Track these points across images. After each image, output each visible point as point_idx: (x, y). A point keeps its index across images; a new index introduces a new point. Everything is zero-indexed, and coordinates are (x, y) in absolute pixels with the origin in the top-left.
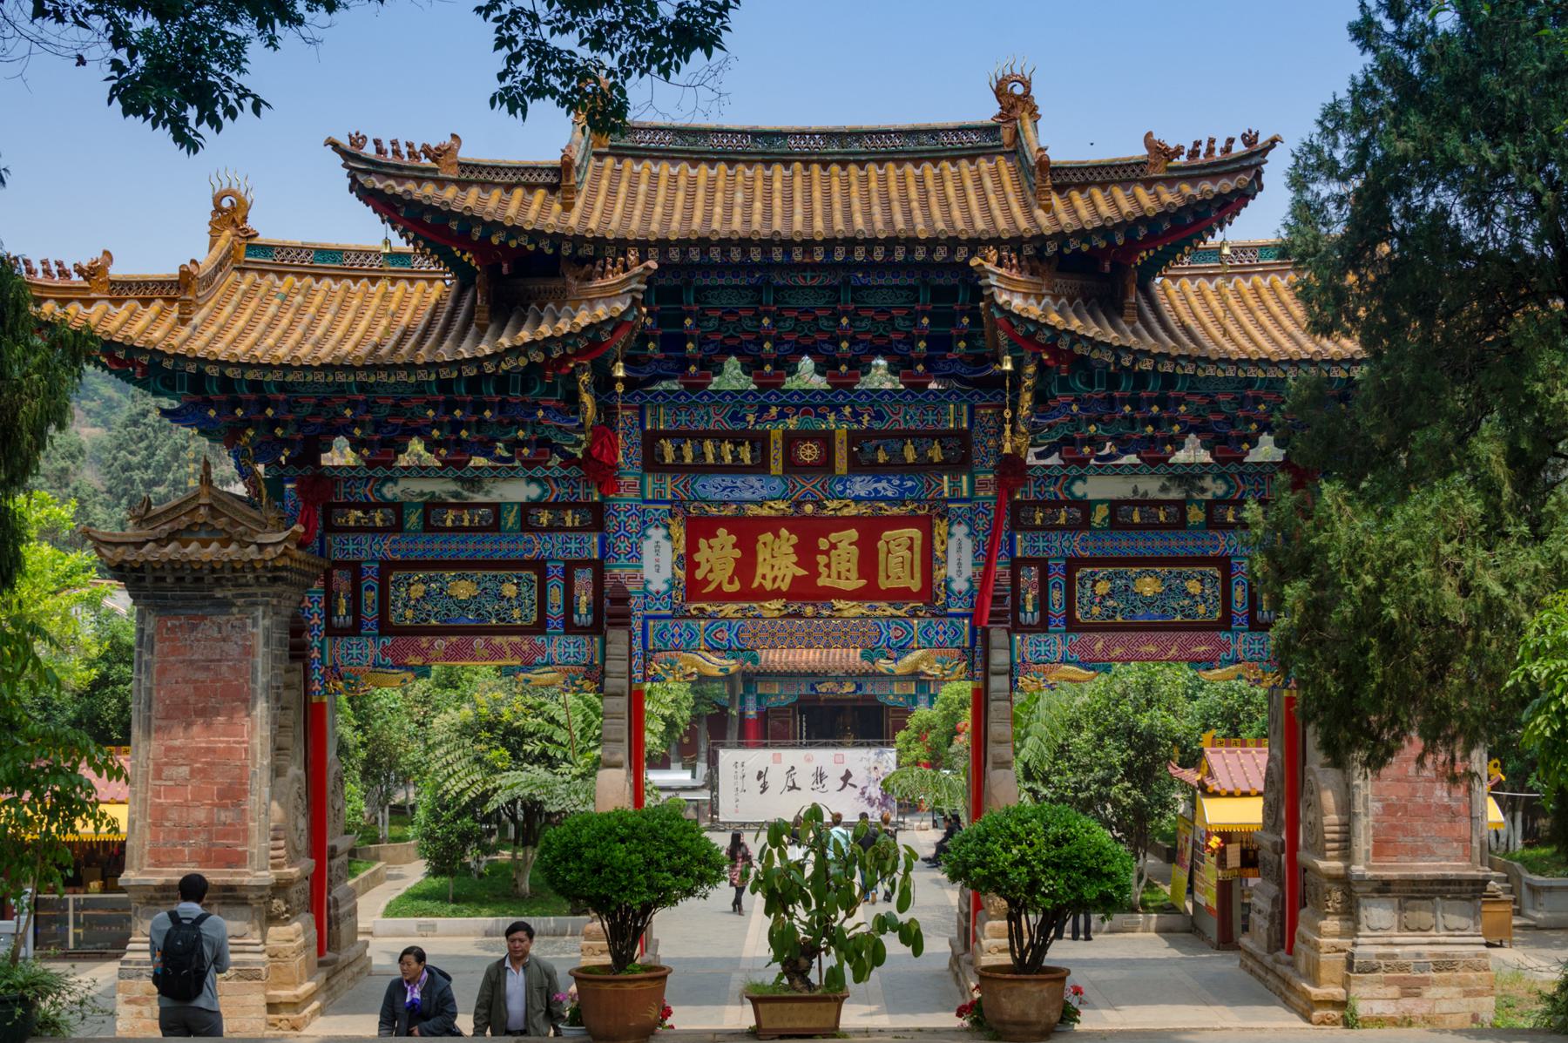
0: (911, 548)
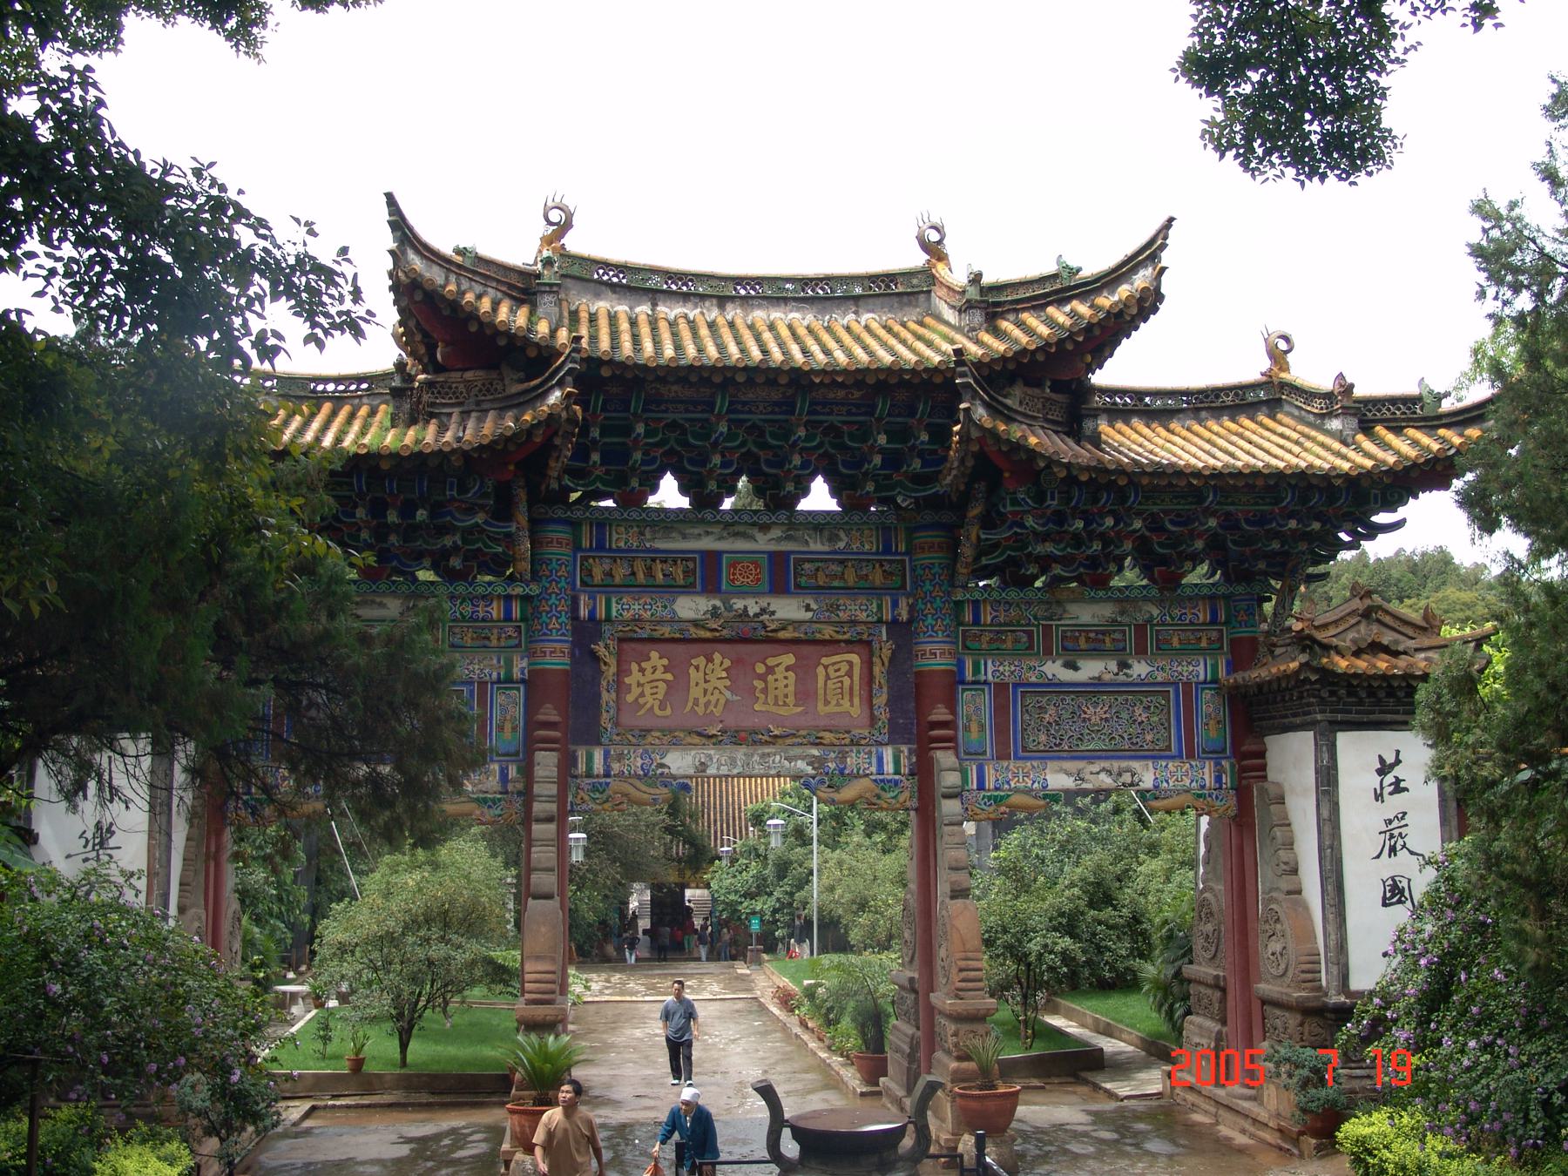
0: (850, 674)
